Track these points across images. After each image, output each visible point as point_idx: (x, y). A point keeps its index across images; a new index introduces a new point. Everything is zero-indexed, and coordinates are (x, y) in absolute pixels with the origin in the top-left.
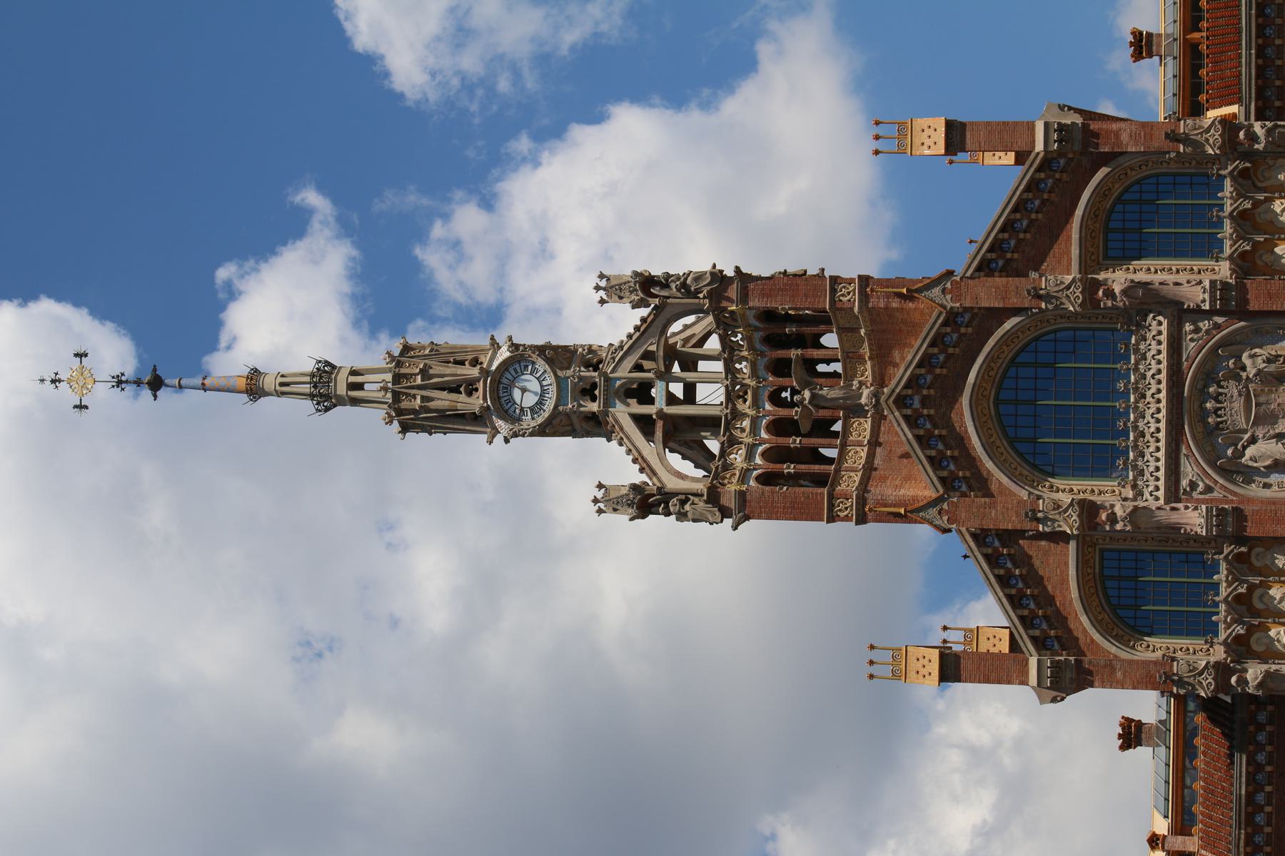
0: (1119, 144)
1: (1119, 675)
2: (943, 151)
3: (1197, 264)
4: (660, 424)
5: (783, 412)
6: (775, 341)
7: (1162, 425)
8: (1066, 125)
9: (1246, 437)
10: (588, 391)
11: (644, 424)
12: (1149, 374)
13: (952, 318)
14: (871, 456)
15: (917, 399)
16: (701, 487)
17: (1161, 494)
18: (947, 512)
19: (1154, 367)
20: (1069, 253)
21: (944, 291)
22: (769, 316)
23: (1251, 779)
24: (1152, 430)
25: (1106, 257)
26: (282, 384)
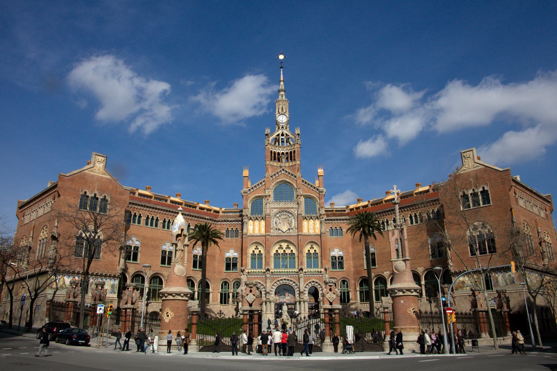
1: (245, 201)
3: (304, 211)
5: (281, 154)
6: (291, 152)
9: (280, 219)
10: (282, 127)
11: (278, 135)
13: (295, 177)
14: (275, 166)
15: (284, 172)
16: (270, 142)
22: (294, 151)
23: (231, 221)
25: (305, 198)
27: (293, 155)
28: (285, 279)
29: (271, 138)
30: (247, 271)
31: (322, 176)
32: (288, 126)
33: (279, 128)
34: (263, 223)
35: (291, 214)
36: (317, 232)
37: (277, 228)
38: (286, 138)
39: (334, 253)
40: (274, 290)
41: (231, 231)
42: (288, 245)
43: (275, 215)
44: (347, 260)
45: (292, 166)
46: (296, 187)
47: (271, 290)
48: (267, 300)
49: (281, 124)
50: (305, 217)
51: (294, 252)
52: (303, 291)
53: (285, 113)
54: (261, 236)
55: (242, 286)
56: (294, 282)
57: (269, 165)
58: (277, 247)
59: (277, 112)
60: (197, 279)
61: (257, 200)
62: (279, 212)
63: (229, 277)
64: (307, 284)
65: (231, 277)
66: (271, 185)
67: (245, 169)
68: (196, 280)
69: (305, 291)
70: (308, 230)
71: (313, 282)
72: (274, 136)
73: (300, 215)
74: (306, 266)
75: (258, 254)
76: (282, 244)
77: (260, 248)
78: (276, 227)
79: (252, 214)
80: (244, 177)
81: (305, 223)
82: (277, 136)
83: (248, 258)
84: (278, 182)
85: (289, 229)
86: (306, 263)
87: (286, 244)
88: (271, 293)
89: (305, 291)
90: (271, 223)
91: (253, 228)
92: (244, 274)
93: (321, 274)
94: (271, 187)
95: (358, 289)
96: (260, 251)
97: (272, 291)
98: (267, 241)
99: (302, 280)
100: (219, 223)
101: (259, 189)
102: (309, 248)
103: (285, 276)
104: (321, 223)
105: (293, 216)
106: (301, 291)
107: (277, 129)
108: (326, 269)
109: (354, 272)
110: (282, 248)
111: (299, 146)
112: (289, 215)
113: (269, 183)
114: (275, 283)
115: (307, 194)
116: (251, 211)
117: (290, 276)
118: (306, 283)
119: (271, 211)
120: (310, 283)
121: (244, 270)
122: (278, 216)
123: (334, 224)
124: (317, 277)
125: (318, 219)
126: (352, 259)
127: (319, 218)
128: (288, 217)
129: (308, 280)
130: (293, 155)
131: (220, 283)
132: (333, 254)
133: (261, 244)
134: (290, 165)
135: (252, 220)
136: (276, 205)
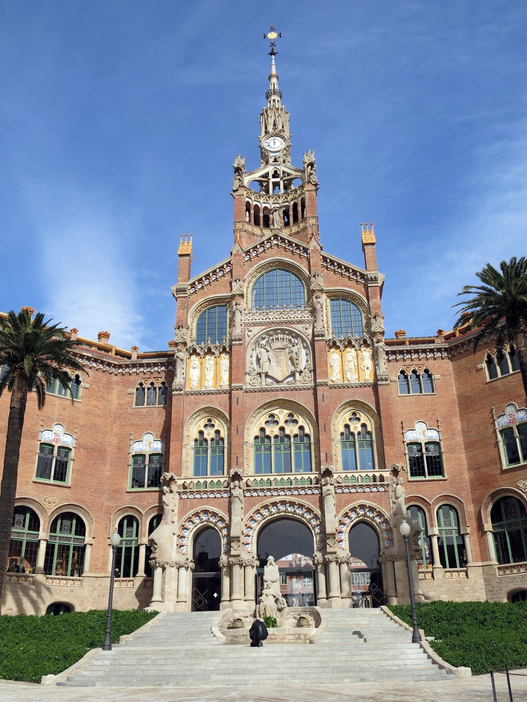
0: (372, 298)
1: (182, 311)
2: (364, 242)
4: (266, 180)
6: (295, 205)
7: (271, 320)
8: (377, 280)
9: (269, 349)
10: (275, 160)
11: (266, 176)
12: (290, 315)
13: (305, 250)
14: (257, 236)
17: (247, 321)
18: (238, 253)
19: (292, 317)
20: (331, 286)
21: (315, 247)
22: (303, 201)
24: (270, 317)
25: (331, 300)
26: (274, 84)
27: (300, 209)
28: (283, 503)
29: (247, 180)
30: (180, 482)
31: (373, 244)
32: (289, 159)
33: (267, 163)
34: (225, 360)
35: (297, 336)
36: (367, 377)
37: (260, 371)
38: (284, 181)
39: (414, 435)
40: (254, 534)
41: (149, 389)
42: (291, 415)
43: (257, 342)
44: (452, 450)
45: (298, 233)
46: (308, 273)
47: (246, 531)
48: (231, 559)
49: (272, 154)
50: (334, 343)
51: (307, 431)
52: (334, 531)
53: (280, 132)
54: (219, 393)
55: (166, 524)
56: (309, 511)
57: (241, 230)
58: (261, 420)
59: (263, 134)
60: (46, 506)
61: (212, 310)
62: (267, 333)
63: (138, 505)
64: (346, 515)
65: (146, 503)
66: (245, 272)
67: (184, 240)
68: (44, 511)
69: (341, 532)
70: (343, 373)
71: (362, 507)
72: (257, 176)
73: (318, 336)
74: (340, 465)
75: (212, 440)
76: (276, 412)
77: (218, 424)
78: (258, 370)
79: (200, 338)
80: (181, 255)
81: (334, 356)
82: (263, 177)
83: (184, 450)
84: (262, 267)
85: (293, 375)
86: (340, 459)
87: (286, 412)
88: (243, 539)
89: (341, 532)
90: (244, 359)
91: (199, 375)
92: (171, 492)
93: (382, 486)
94: (245, 277)
95: (488, 526)
96: (218, 432)
97: (248, 536)
98: (234, 404)
99: (330, 502)
100: (121, 370)
101: (216, 283)
102: (348, 419)
103: (282, 493)
104: (375, 357)
105: (303, 341)
106: (329, 530)
107: (263, 165)
108: (395, 472)
109: (472, 482)
110: (277, 422)
111: (314, 188)
112: (293, 340)
113: (241, 267)
114: (258, 512)
115: (338, 288)
116: (198, 335)
117: (296, 493)
118: (343, 512)
119: (247, 332)
120: (353, 510)
121: (172, 479)
122: (264, 342)
123: (408, 362)
124: (371, 494)
125: (368, 346)
126: (465, 448)
127: (369, 342)
128: (290, 345)
129: (347, 503)
130: (300, 209)
131: (115, 520)
132: (410, 436)
133: (219, 414)
134: (293, 231)
135: (198, 354)
136: (258, 318)
